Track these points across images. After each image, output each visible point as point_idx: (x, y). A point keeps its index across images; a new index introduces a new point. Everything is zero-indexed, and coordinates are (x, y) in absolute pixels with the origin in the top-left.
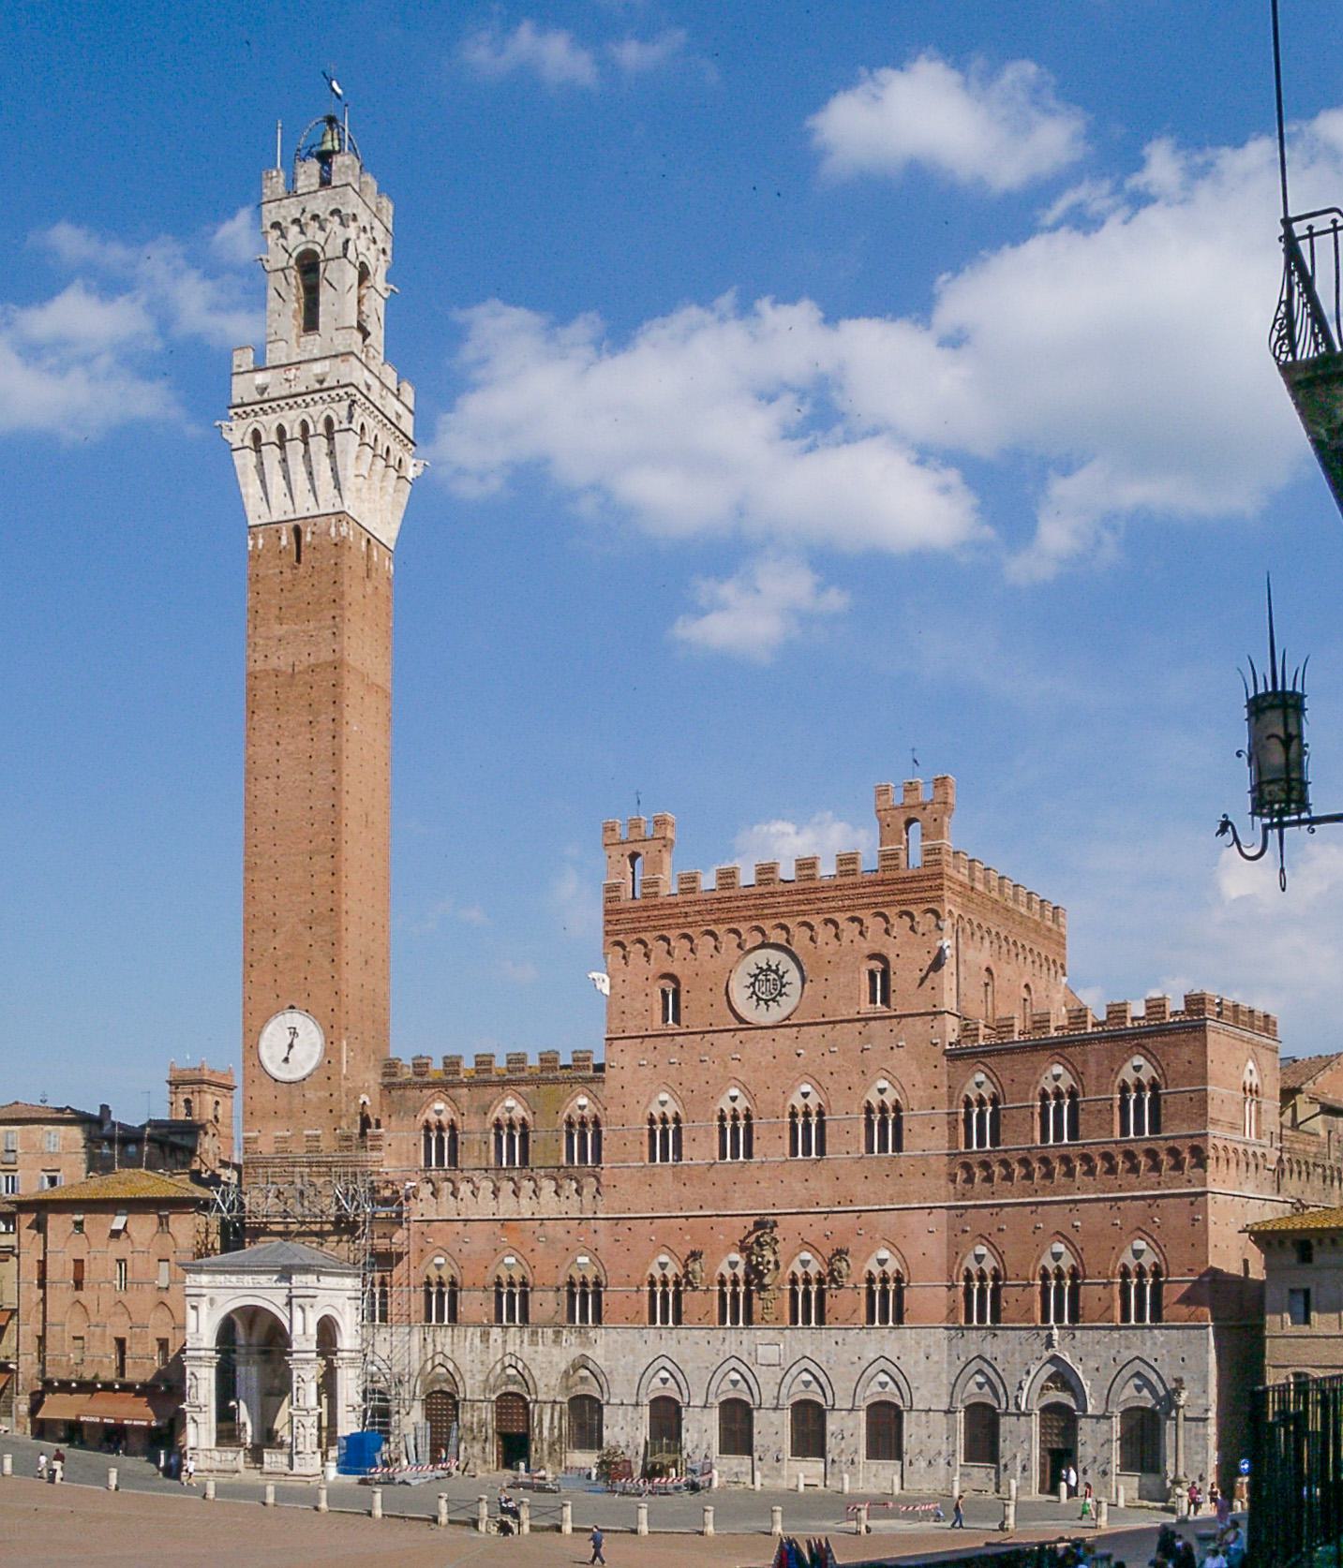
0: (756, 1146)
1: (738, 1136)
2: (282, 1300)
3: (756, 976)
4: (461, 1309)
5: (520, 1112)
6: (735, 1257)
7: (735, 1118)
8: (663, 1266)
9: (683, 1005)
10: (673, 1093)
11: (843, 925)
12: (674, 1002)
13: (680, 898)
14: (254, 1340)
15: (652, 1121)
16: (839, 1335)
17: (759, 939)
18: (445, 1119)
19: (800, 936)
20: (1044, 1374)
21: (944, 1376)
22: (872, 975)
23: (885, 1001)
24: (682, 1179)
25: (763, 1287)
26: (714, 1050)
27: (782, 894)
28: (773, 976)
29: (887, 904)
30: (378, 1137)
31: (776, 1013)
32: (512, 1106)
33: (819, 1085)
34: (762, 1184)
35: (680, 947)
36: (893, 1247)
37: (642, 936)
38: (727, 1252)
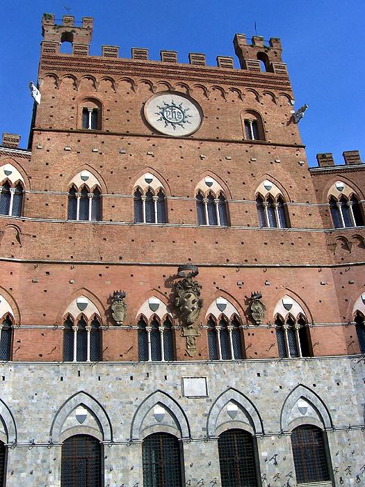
0: (171, 215)
6: (155, 300)
8: (82, 306)
9: (104, 117)
10: (94, 172)
13: (106, 58)
19: (197, 94)
21: (354, 399)
22: (247, 122)
24: (103, 234)
25: (187, 324)
27: (182, 68)
28: (177, 110)
33: (219, 179)
34: (177, 244)
37: (71, 73)
38: (147, 297)
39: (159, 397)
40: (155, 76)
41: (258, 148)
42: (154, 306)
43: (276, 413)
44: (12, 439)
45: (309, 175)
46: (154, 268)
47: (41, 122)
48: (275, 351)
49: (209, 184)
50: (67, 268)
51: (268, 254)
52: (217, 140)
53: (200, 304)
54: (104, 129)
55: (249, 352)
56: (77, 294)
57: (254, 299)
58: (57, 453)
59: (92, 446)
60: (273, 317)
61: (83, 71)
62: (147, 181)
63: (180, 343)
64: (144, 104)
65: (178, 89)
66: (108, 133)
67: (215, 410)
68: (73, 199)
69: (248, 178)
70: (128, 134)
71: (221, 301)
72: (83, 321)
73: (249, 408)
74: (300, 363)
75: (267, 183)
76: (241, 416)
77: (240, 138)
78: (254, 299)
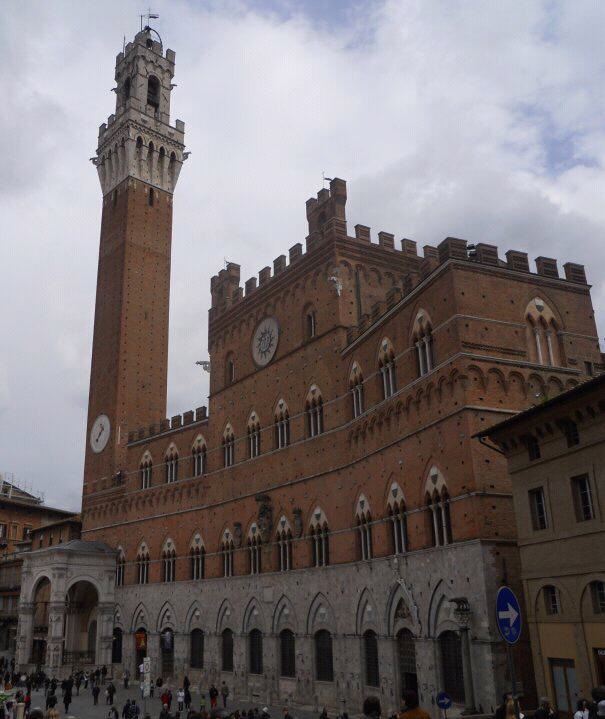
3: (260, 340)
14: (75, 600)
17: (261, 316)
20: (395, 604)
31: (270, 356)
32: (172, 448)
41: (310, 349)
42: (253, 531)
48: (306, 562)
57: (298, 512)
60: (307, 532)
64: (252, 337)
65: (269, 311)
77: (299, 344)
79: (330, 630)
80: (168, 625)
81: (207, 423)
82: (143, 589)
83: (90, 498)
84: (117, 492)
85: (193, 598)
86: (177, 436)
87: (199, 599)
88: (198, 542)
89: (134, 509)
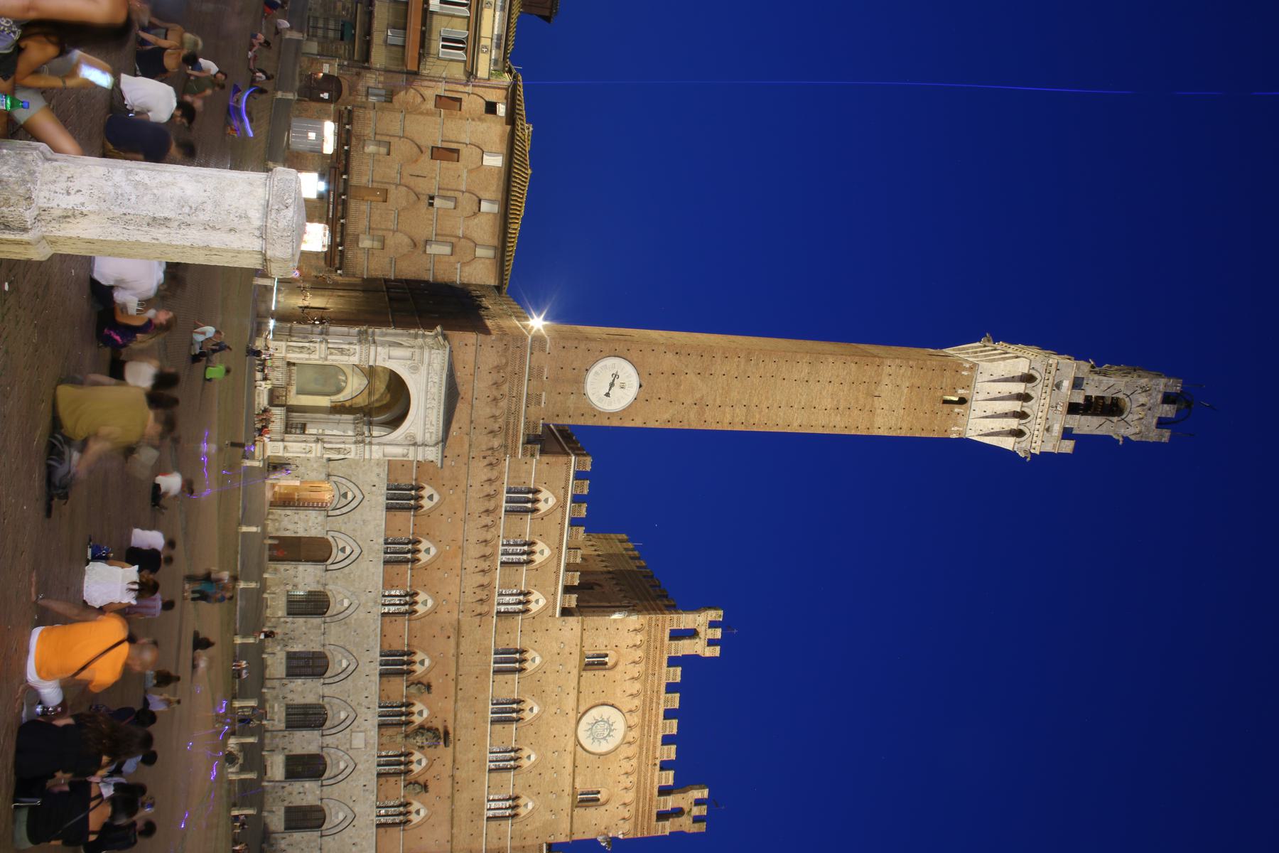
0: (498, 727)
1: (508, 713)
2: (413, 430)
3: (607, 722)
4: (398, 513)
5: (538, 558)
7: (518, 711)
8: (422, 663)
11: (631, 778)
12: (596, 663)
15: (522, 652)
16: (373, 784)
18: (540, 505)
23: (582, 801)
25: (407, 736)
26: (564, 695)
29: (638, 803)
30: (533, 455)
33: (535, 766)
35: (635, 670)
36: (427, 818)
38: (429, 708)
39: (352, 715)
40: (644, 714)
41: (567, 801)
42: (421, 713)
43: (335, 796)
44: (328, 620)
45: (539, 841)
46: (451, 715)
47: (594, 621)
49: (530, 758)
50: (452, 651)
51: (463, 798)
52: (575, 766)
53: (421, 748)
54: (584, 674)
55: (383, 780)
56: (432, 659)
58: (318, 648)
59: (318, 670)
61: (648, 654)
62: (532, 709)
63: (391, 731)
64: (612, 706)
66: (580, 676)
67: (341, 754)
68: (516, 651)
69: (536, 790)
70: (579, 692)
71: (424, 763)
72: (411, 663)
73: (340, 777)
74: (373, 817)
75: (530, 806)
76: (335, 772)
77: (577, 785)
78: (425, 787)
79: (324, 827)
80: (335, 551)
81: (553, 616)
82: (382, 500)
83: (522, 357)
84: (516, 435)
85: (363, 599)
86: (555, 561)
87: (361, 608)
88: (425, 602)
89: (484, 474)
